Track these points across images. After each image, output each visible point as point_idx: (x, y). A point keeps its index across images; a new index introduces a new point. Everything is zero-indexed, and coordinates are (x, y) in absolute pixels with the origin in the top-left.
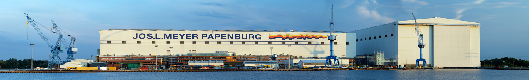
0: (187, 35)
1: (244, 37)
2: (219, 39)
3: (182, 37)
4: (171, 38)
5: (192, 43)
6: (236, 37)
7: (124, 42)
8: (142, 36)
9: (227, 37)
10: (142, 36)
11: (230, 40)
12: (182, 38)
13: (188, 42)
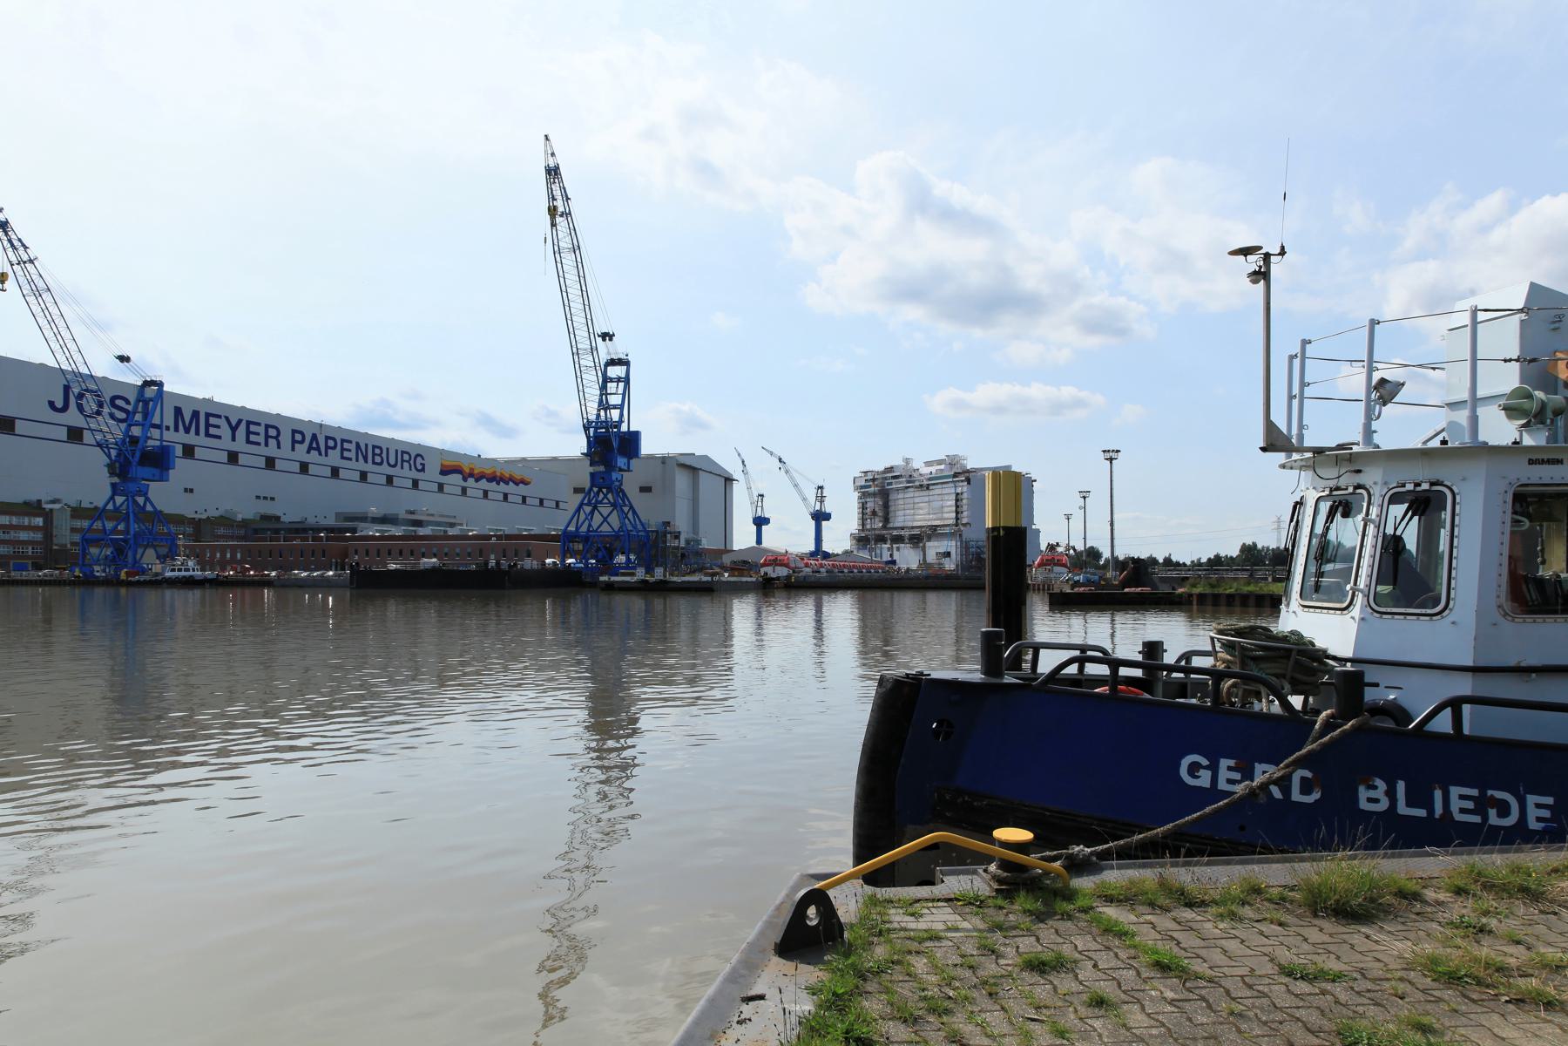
0: (249, 423)
1: (392, 461)
3: (234, 429)
4: (197, 433)
5: (262, 462)
6: (374, 454)
8: (90, 404)
9: (352, 455)
10: (90, 404)
11: (361, 465)
12: (234, 439)
13: (252, 456)
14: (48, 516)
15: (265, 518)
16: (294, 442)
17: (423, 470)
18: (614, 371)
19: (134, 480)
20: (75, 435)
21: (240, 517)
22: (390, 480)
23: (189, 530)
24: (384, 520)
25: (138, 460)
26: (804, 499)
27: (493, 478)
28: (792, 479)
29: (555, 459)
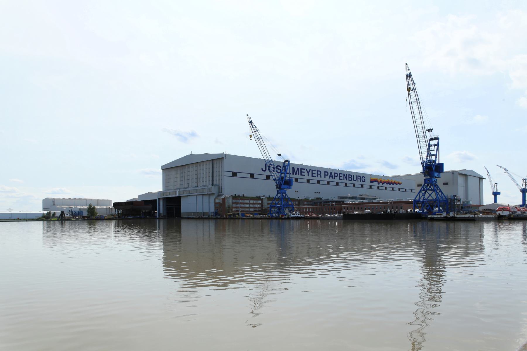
0: (312, 170)
1: (355, 179)
2: (337, 180)
3: (308, 173)
5: (316, 182)
7: (252, 176)
8: (271, 169)
9: (342, 178)
10: (271, 169)
11: (345, 181)
13: (313, 180)
14: (262, 200)
15: (317, 199)
16: (325, 175)
17: (365, 181)
18: (432, 143)
19: (282, 189)
20: (268, 177)
21: (310, 199)
22: (354, 185)
23: (297, 203)
24: (353, 198)
25: (284, 184)
26: (517, 184)
27: (389, 183)
28: (511, 176)
29: (410, 175)
